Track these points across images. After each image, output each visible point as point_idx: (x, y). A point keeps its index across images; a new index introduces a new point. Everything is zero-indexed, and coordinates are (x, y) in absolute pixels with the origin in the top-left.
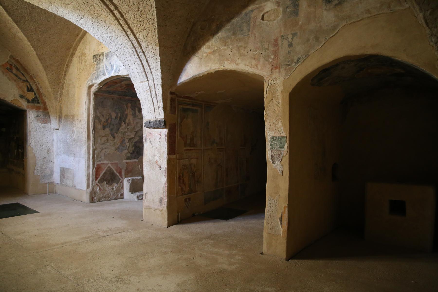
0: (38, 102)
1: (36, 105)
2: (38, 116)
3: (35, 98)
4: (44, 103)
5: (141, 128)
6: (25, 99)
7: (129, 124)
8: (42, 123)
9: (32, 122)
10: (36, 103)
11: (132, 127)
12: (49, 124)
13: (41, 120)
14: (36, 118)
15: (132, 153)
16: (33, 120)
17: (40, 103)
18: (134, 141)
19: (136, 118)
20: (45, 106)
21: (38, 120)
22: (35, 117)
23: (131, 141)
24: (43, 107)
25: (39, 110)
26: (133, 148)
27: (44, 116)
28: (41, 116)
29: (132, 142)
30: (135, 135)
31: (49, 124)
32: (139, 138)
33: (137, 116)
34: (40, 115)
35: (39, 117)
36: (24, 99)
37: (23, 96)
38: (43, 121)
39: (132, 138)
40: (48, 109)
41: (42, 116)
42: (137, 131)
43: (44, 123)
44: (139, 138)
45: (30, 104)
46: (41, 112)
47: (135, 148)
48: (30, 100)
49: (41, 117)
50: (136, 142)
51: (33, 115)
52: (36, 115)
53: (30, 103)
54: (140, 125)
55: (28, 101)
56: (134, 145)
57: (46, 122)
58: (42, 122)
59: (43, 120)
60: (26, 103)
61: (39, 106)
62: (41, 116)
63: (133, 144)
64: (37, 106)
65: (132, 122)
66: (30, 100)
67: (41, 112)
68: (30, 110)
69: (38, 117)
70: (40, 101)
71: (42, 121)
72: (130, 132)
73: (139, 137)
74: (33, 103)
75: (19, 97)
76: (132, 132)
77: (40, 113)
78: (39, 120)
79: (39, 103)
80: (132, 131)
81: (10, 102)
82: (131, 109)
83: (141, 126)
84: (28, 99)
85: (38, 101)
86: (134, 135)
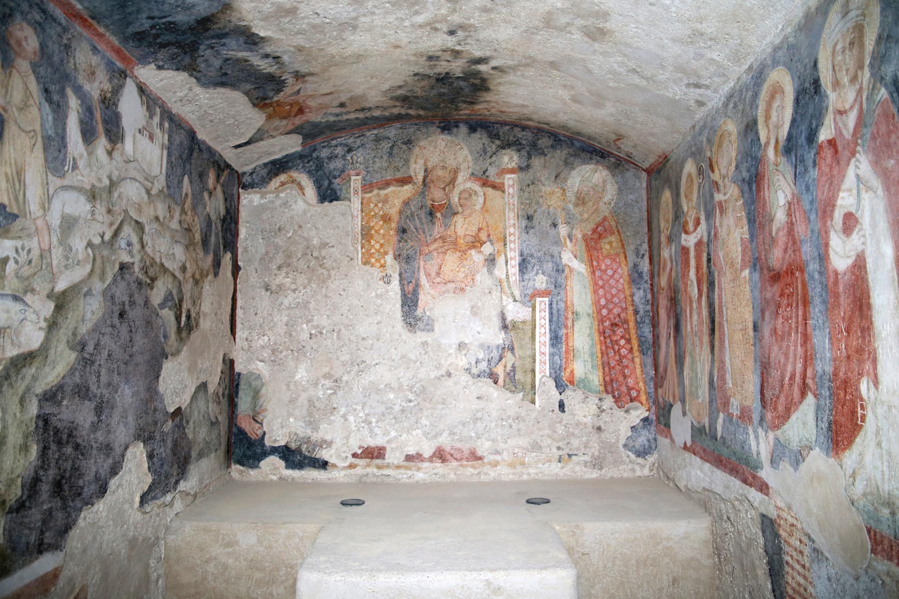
5: (88, 268)
7: (15, 217)
11: (36, 253)
15: (21, 506)
18: (40, 388)
19: (66, 182)
23: (21, 387)
26: (34, 450)
29: (28, 389)
30: (52, 325)
32: (73, 356)
33: (75, 167)
39: (28, 358)
42: (64, 293)
44: (73, 356)
47: (44, 451)
50: (51, 397)
54: (85, 243)
56: (38, 417)
63: (33, 409)
65: (34, 207)
72: (16, 298)
73: (72, 348)
76: (28, 298)
80: (33, 291)
82: (34, 86)
83: (89, 250)
86: (43, 324)
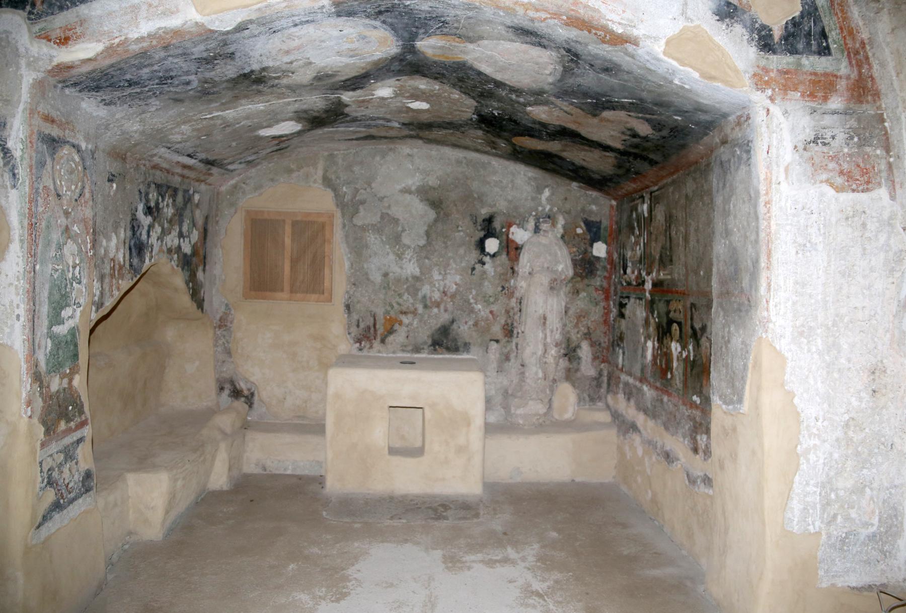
0: (819, 45)
1: (812, 63)
2: (815, 141)
3: (802, 16)
4: (857, 53)
6: (745, 26)
8: (839, 189)
9: (782, 177)
10: (808, 50)
12: (882, 192)
13: (832, 165)
14: (807, 155)
16: (787, 170)
17: (833, 47)
20: (860, 73)
21: (816, 167)
22: (801, 146)
24: (848, 78)
25: (825, 99)
27: (852, 138)
28: (833, 137)
31: (882, 192)
34: (829, 135)
35: (825, 149)
36: (738, 29)
37: (736, 8)
38: (848, 175)
40: (877, 95)
41: (841, 137)
43: (853, 191)
45: (774, 58)
46: (834, 113)
48: (777, 33)
49: (835, 144)
51: (792, 130)
52: (808, 130)
53: (774, 52)
55: (766, 43)
57: (868, 182)
58: (839, 180)
59: (845, 166)
60: (752, 52)
61: (826, 75)
62: (833, 137)
64: (815, 74)
66: (777, 33)
67: (834, 113)
68: (772, 99)
69: (819, 148)
70: (833, 35)
71: (841, 173)
74: (793, 51)
75: (709, 13)
77: (828, 120)
78: (825, 168)
79: (825, 51)
81: (659, 48)
84: (764, 27)
85: (824, 35)
